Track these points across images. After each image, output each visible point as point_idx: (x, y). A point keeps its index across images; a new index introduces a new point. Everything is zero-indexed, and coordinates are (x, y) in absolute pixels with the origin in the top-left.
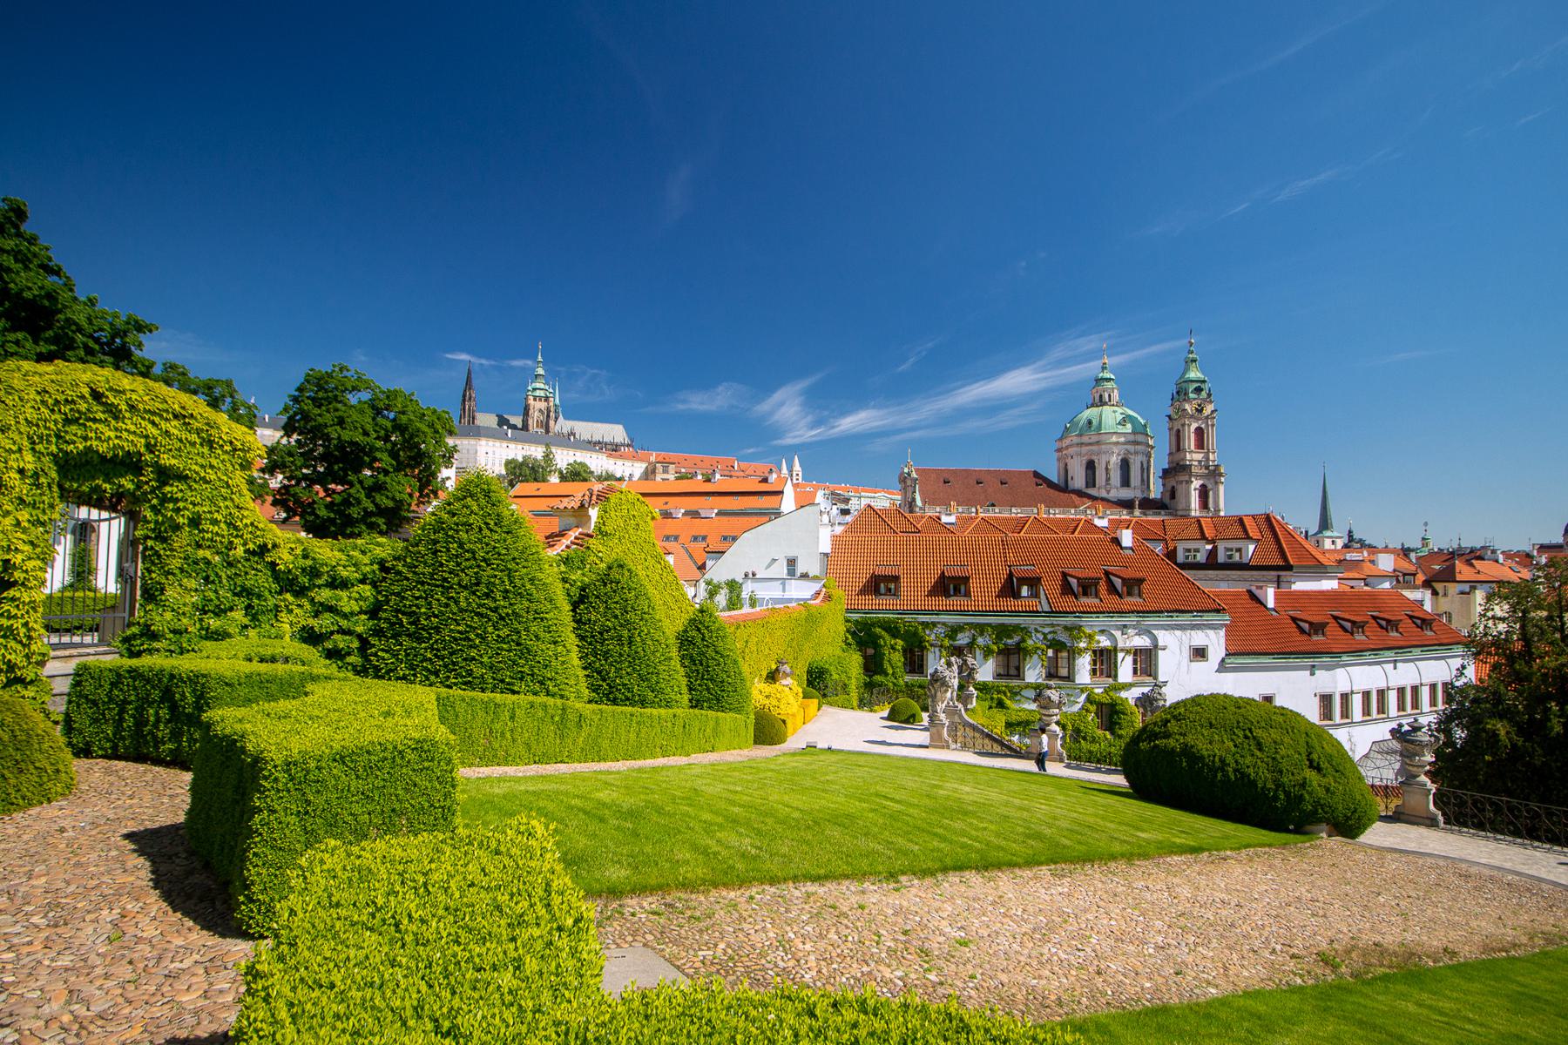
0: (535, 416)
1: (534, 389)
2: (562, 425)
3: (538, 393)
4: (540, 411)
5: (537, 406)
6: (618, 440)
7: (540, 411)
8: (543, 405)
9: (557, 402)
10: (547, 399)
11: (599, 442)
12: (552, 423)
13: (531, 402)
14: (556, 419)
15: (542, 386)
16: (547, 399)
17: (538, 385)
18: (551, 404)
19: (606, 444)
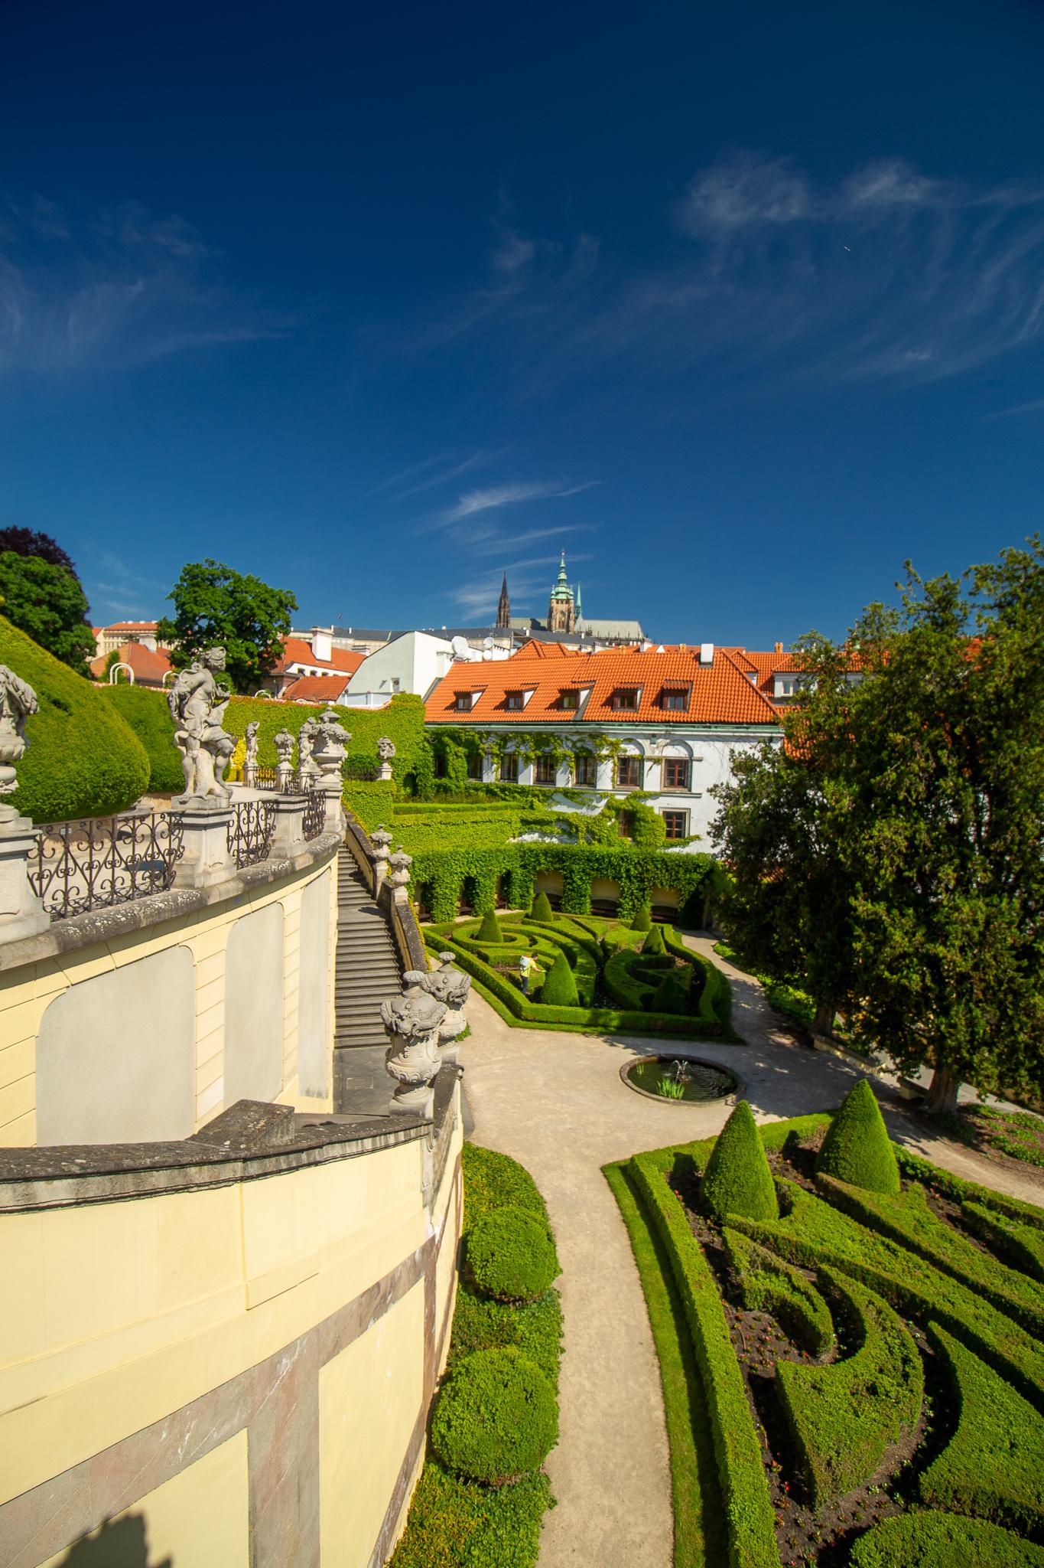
0: (558, 617)
1: (557, 593)
2: (582, 625)
3: (561, 596)
4: (562, 612)
5: (559, 608)
6: (633, 636)
7: (562, 612)
8: (564, 607)
9: (579, 603)
10: (568, 601)
11: (616, 639)
12: (571, 623)
13: (554, 604)
14: (576, 618)
15: (564, 590)
16: (568, 601)
17: (561, 589)
18: (572, 605)
19: (621, 640)
